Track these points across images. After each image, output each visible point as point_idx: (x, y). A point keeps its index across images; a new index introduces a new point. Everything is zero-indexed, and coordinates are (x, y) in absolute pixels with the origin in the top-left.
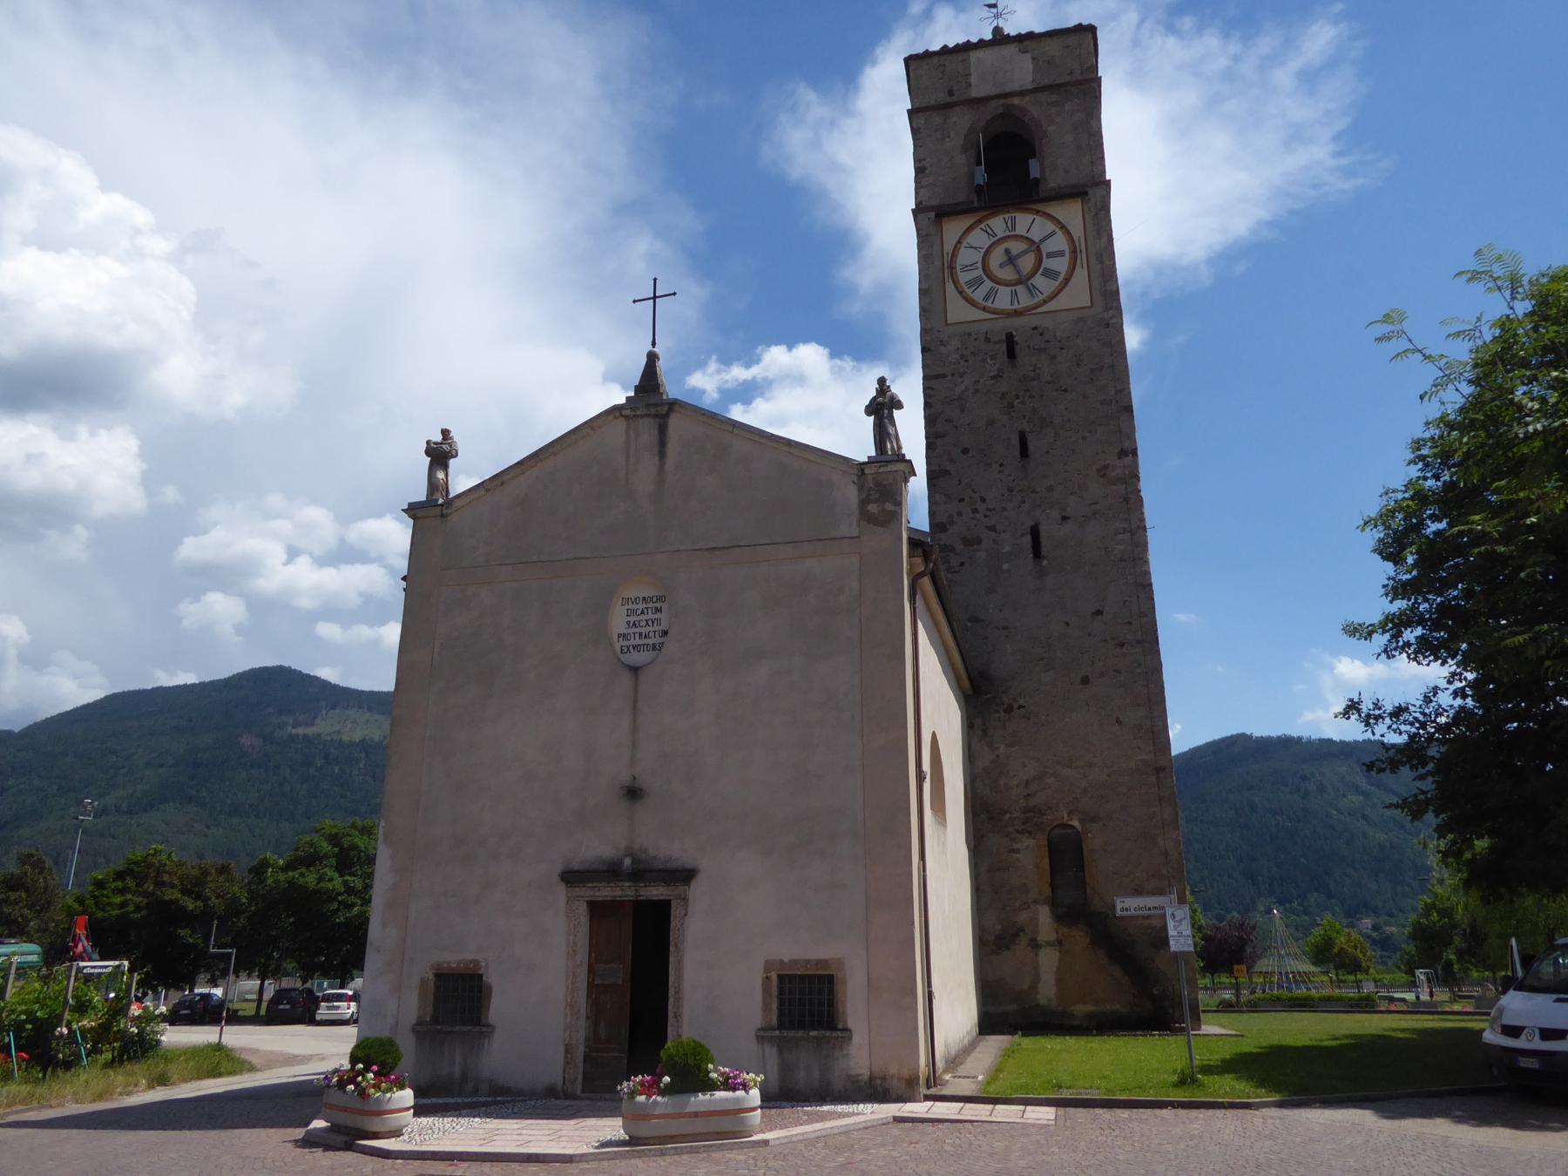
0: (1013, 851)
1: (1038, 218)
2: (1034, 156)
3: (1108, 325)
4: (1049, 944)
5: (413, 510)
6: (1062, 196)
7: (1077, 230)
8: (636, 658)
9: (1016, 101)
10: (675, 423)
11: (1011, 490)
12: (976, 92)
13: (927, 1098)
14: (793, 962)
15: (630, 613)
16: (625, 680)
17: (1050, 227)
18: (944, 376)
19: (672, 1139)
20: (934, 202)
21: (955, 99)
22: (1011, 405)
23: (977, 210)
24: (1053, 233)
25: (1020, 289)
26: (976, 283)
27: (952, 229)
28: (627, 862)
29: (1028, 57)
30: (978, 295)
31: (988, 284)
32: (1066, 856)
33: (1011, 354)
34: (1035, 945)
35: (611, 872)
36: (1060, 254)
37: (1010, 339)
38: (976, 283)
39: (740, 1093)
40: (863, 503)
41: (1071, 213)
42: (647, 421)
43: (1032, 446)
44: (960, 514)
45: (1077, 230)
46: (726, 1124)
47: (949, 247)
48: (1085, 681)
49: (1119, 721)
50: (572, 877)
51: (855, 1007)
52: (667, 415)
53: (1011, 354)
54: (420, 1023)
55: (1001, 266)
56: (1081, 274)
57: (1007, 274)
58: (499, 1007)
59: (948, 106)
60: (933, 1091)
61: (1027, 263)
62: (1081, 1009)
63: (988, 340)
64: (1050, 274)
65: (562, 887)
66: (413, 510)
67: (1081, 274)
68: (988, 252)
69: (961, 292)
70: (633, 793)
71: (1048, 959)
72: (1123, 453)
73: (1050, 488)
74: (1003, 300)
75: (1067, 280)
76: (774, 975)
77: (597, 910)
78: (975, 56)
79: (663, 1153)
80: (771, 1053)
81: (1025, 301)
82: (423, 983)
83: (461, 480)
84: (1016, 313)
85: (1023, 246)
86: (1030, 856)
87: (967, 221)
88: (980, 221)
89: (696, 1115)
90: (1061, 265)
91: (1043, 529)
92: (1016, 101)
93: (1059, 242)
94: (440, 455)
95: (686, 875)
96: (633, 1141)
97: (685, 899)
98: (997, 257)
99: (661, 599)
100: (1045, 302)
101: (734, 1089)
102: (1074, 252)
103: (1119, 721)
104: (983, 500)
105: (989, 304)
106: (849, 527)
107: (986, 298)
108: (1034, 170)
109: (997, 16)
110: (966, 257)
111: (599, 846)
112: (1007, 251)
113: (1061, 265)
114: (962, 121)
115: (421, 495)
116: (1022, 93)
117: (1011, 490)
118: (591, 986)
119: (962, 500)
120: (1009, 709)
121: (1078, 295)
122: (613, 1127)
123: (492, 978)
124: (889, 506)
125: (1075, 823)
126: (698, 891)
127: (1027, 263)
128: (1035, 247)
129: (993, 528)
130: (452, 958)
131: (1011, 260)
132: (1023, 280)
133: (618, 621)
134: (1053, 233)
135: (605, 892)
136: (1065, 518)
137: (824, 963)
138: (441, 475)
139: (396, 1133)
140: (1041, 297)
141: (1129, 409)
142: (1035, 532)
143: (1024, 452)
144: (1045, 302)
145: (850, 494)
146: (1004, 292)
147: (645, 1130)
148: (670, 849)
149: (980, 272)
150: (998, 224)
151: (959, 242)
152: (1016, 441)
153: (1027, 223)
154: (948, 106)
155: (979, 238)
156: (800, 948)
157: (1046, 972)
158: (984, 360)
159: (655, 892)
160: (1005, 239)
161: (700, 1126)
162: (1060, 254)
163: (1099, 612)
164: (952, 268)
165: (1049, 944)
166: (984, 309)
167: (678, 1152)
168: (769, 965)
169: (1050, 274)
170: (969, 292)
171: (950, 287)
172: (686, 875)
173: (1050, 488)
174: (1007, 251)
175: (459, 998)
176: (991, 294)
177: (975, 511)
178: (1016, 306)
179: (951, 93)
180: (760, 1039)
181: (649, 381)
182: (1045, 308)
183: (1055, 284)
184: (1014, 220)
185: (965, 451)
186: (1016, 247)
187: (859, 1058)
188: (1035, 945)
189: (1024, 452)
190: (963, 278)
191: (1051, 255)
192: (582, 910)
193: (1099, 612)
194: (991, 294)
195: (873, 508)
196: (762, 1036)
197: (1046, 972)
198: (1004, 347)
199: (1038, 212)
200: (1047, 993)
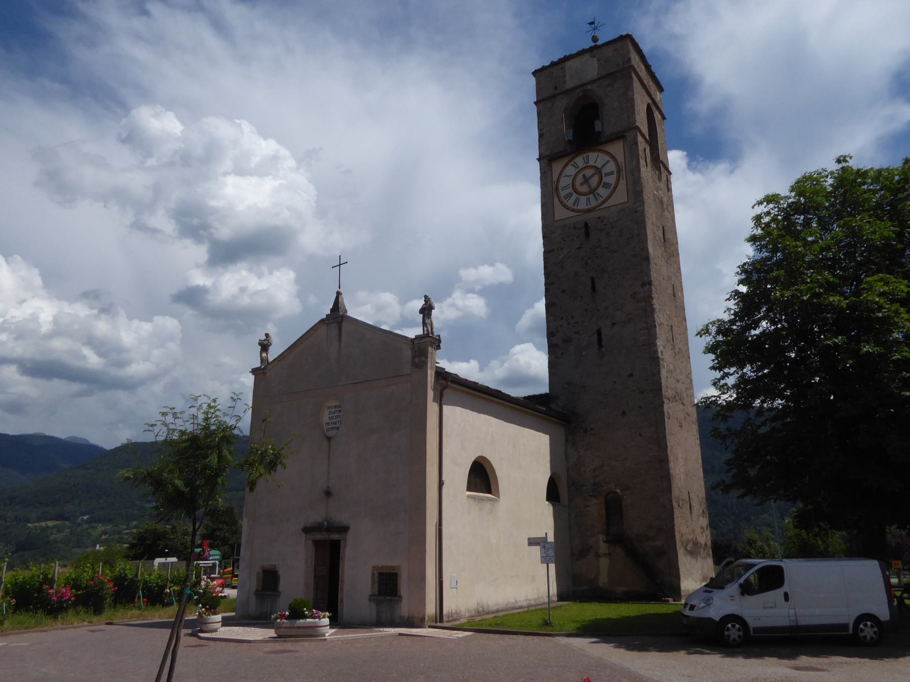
0: (589, 506)
1: (601, 155)
2: (598, 118)
3: (636, 212)
4: (605, 555)
5: (254, 371)
6: (612, 139)
7: (621, 159)
9: (589, 87)
10: (345, 326)
11: (586, 311)
12: (569, 86)
13: (430, 627)
14: (382, 567)
15: (330, 413)
17: (607, 158)
18: (553, 251)
19: (290, 636)
20: (548, 153)
21: (558, 92)
22: (586, 263)
23: (568, 155)
24: (608, 162)
25: (591, 196)
26: (569, 195)
27: (557, 167)
28: (325, 523)
29: (595, 59)
30: (570, 203)
31: (575, 196)
32: (613, 508)
33: (587, 234)
34: (598, 556)
35: (318, 528)
36: (612, 173)
37: (586, 224)
38: (569, 195)
39: (317, 620)
40: (413, 358)
41: (617, 149)
42: (334, 325)
43: (597, 285)
44: (561, 326)
45: (621, 159)
46: (310, 632)
47: (555, 178)
48: (624, 413)
49: (641, 435)
50: (307, 530)
51: (404, 588)
52: (342, 322)
53: (587, 234)
54: (257, 590)
55: (582, 184)
56: (623, 183)
57: (584, 189)
58: (283, 585)
59: (554, 96)
60: (439, 624)
61: (594, 181)
62: (621, 589)
63: (575, 228)
64: (606, 186)
65: (303, 535)
66: (254, 371)
67: (623, 183)
68: (575, 177)
69: (561, 203)
70: (328, 493)
71: (604, 563)
72: (644, 285)
73: (606, 308)
74: (582, 205)
75: (615, 188)
76: (376, 573)
77: (317, 543)
78: (568, 64)
79: (285, 641)
80: (374, 606)
81: (594, 203)
82: (258, 574)
83: (273, 354)
84: (589, 211)
85: (592, 171)
86: (595, 509)
87: (566, 160)
88: (571, 160)
89: (299, 628)
90: (611, 180)
91: (603, 331)
92: (589, 87)
93: (611, 167)
94: (265, 346)
95: (344, 529)
96: (279, 637)
97: (345, 540)
98: (580, 179)
99: (340, 406)
100: (604, 202)
101: (315, 618)
102: (619, 171)
103: (641, 435)
104: (573, 317)
105: (575, 207)
106: (407, 369)
107: (574, 205)
108: (598, 126)
109: (595, 29)
110: (565, 181)
111: (315, 517)
112: (584, 176)
113: (611, 180)
114: (562, 103)
115: (257, 364)
116: (592, 82)
117: (586, 311)
118: (316, 577)
119: (562, 318)
120: (586, 431)
121: (621, 196)
122: (272, 633)
123: (280, 573)
124: (423, 359)
125: (618, 491)
126: (350, 536)
127: (594, 181)
128: (598, 171)
129: (577, 333)
131: (586, 180)
132: (592, 191)
133: (326, 418)
134: (608, 162)
135: (318, 536)
136: (614, 324)
137: (393, 568)
138: (264, 355)
139: (215, 631)
140: (602, 200)
142: (599, 333)
144: (604, 202)
145: (408, 354)
146: (583, 199)
147: (283, 632)
148: (341, 518)
149: (571, 190)
150: (580, 161)
151: (560, 174)
152: (589, 283)
153: (595, 158)
154: (554, 96)
155: (570, 170)
157: (603, 569)
158: (573, 239)
159: (335, 536)
160: (584, 168)
161: (300, 632)
162: (612, 173)
163: (631, 375)
164: (557, 189)
165: (605, 555)
166: (573, 210)
167: (290, 641)
168: (374, 568)
169: (606, 186)
170: (565, 201)
171: (556, 200)
172: (344, 529)
173: (606, 308)
174: (584, 176)
175: (269, 580)
176: (577, 201)
177: (569, 324)
178: (589, 207)
179: (556, 88)
180: (370, 600)
181: (337, 306)
182: (604, 206)
183: (609, 191)
184: (588, 157)
185: (564, 291)
186: (589, 173)
187: (405, 609)
188: (598, 556)
190: (563, 193)
191: (607, 175)
192: (310, 543)
193: (631, 375)
194: (577, 201)
195: (417, 360)
196: (372, 598)
197: (603, 569)
198: (583, 231)
199: (600, 151)
200: (603, 580)
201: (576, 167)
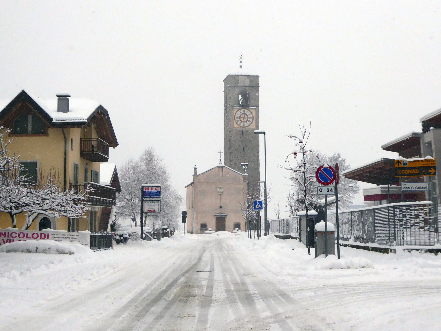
8: (221, 194)
16: (219, 196)
17: (250, 113)
26: (238, 121)
30: (238, 123)
31: (240, 121)
33: (243, 134)
36: (251, 118)
38: (238, 121)
53: (243, 134)
56: (254, 123)
67: (254, 123)
70: (221, 207)
74: (242, 125)
81: (246, 125)
84: (244, 127)
111: (218, 211)
123: (207, 224)
130: (203, 222)
131: (244, 118)
135: (218, 216)
141: (259, 146)
143: (244, 151)
150: (242, 111)
156: (237, 221)
159: (223, 216)
162: (251, 118)
171: (234, 121)
189: (244, 151)
190: (236, 119)
194: (240, 123)
201: (241, 112)
